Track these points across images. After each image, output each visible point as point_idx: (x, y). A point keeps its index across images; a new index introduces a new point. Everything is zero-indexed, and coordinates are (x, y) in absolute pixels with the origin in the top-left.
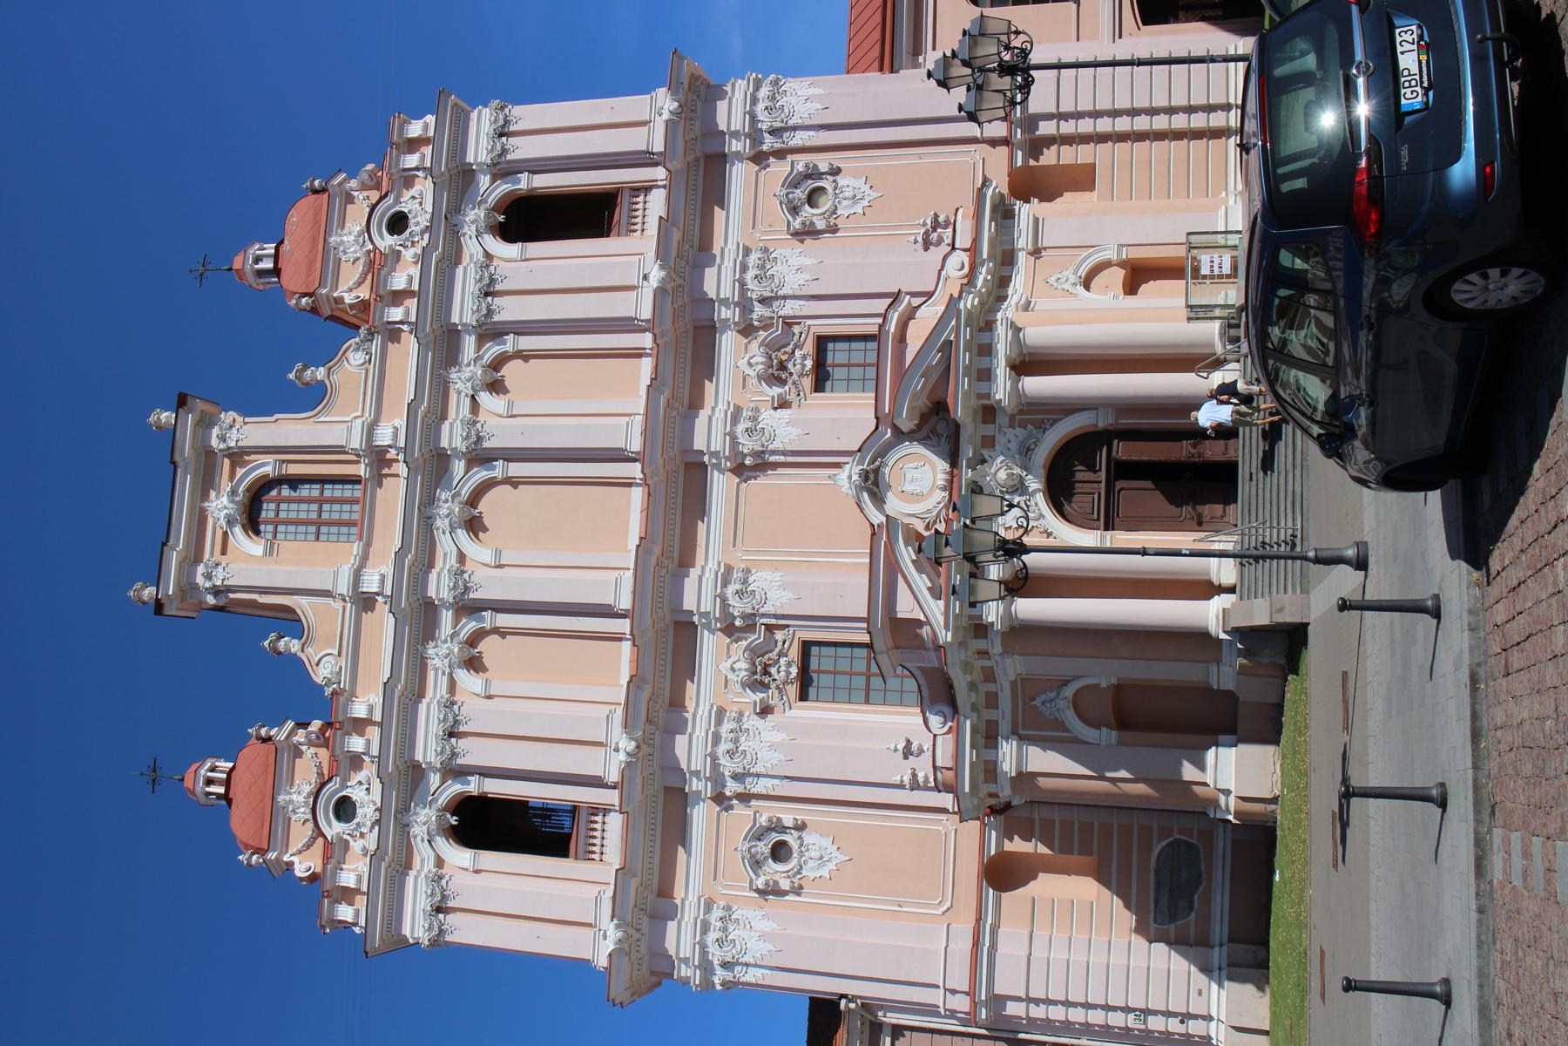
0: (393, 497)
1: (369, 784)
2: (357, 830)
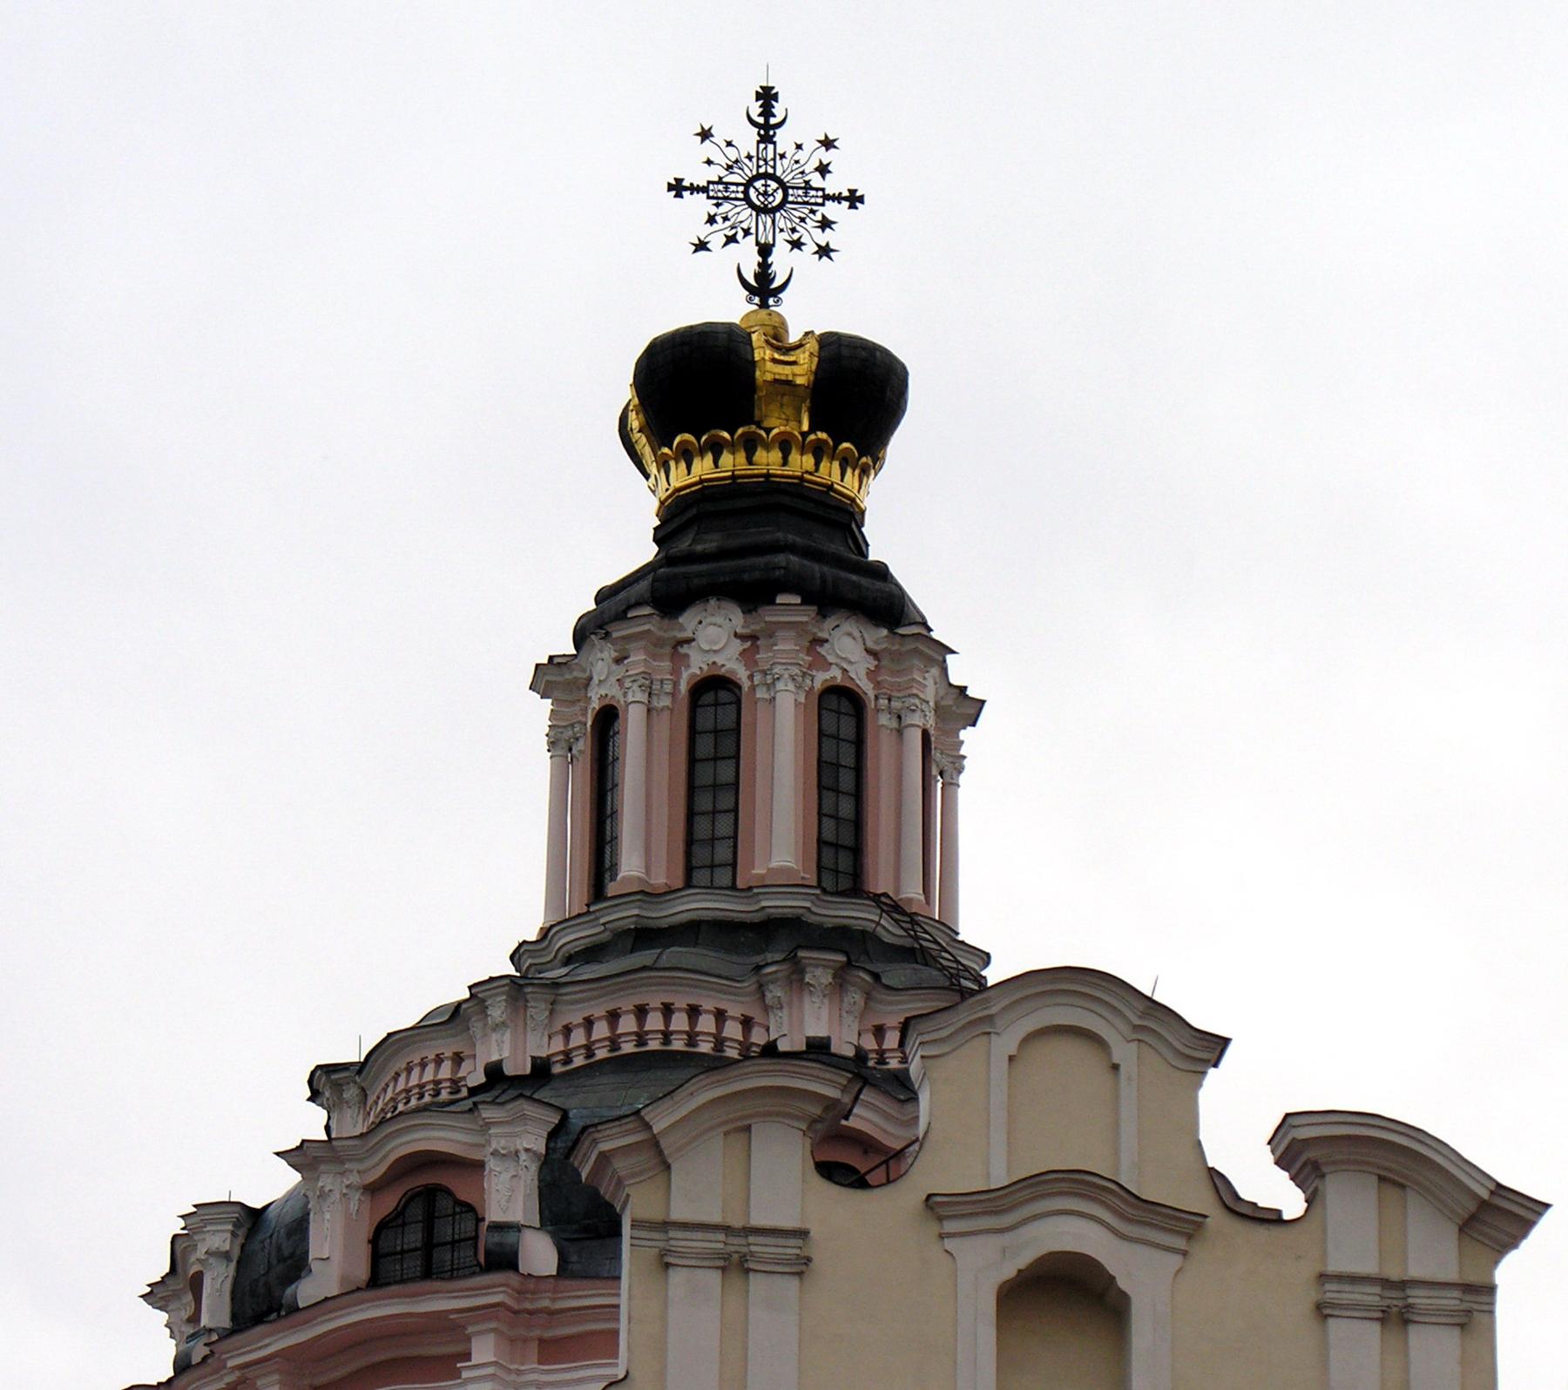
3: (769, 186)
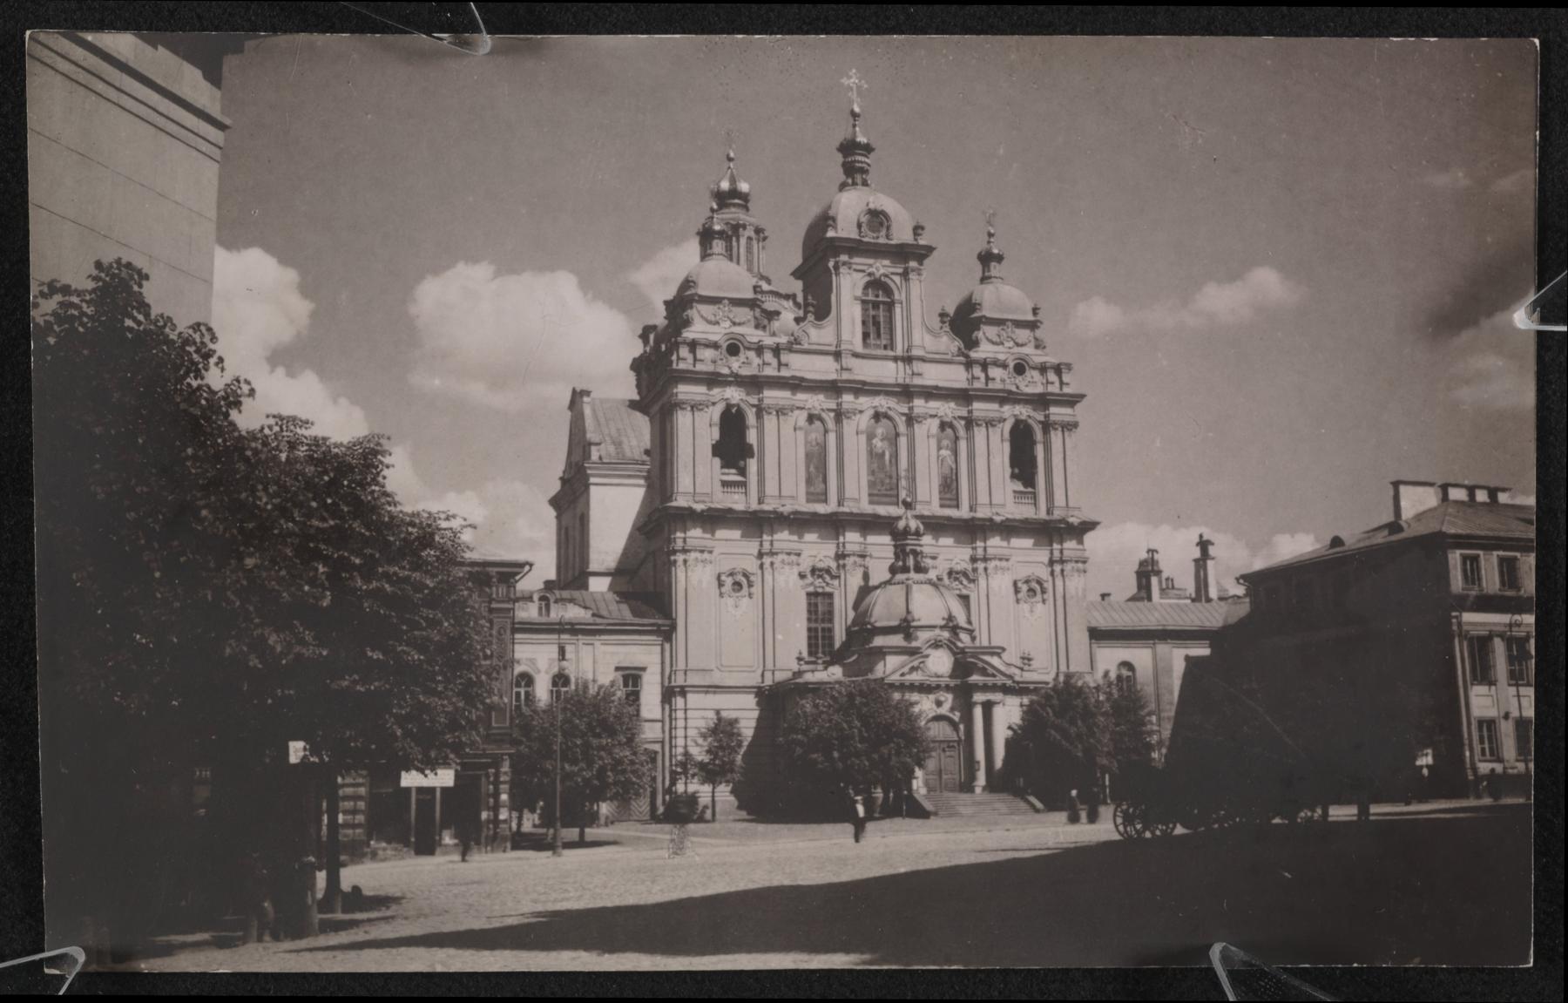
0: (887, 372)
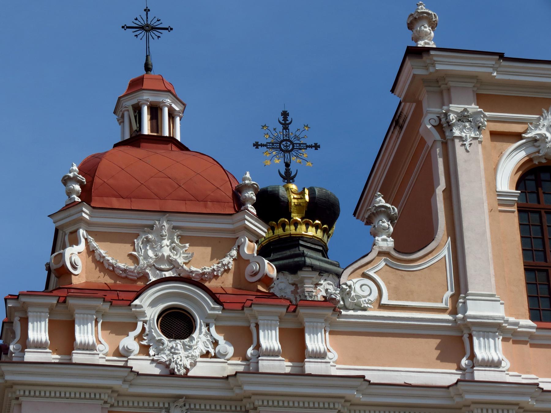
1: (215, 357)
2: (150, 341)
3: (288, 143)
